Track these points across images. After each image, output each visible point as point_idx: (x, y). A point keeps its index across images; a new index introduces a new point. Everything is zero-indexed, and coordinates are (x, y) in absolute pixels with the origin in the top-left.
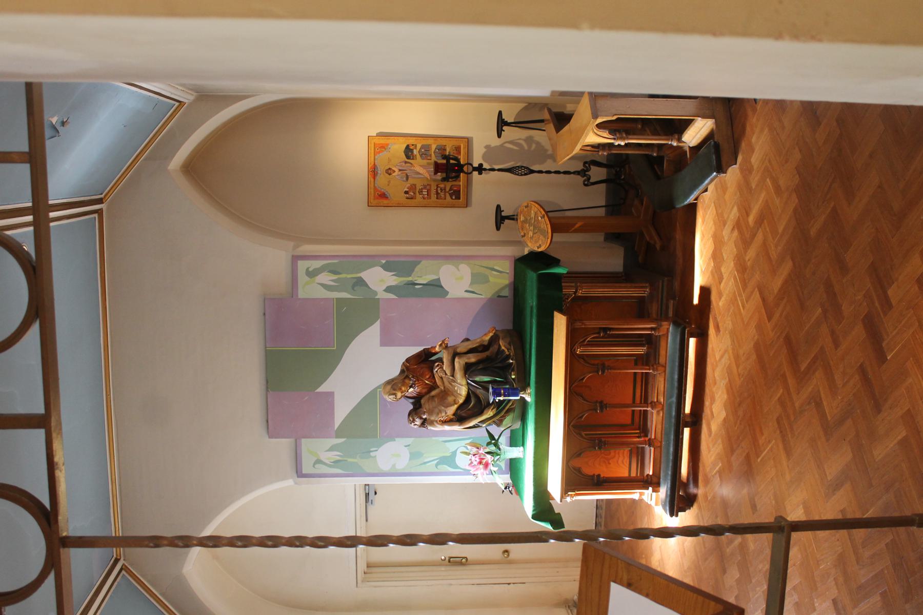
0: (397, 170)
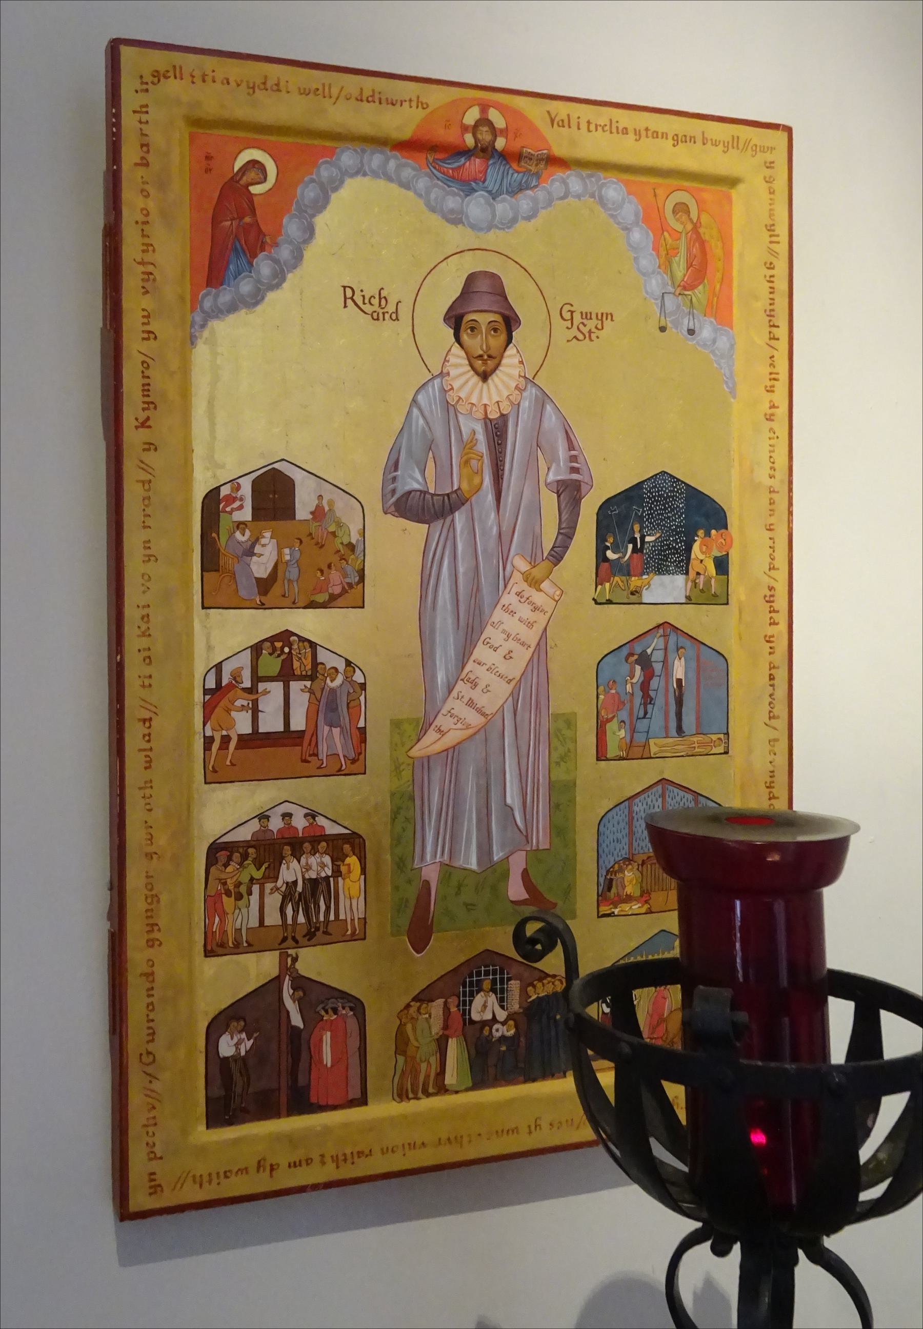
0: (499, 391)
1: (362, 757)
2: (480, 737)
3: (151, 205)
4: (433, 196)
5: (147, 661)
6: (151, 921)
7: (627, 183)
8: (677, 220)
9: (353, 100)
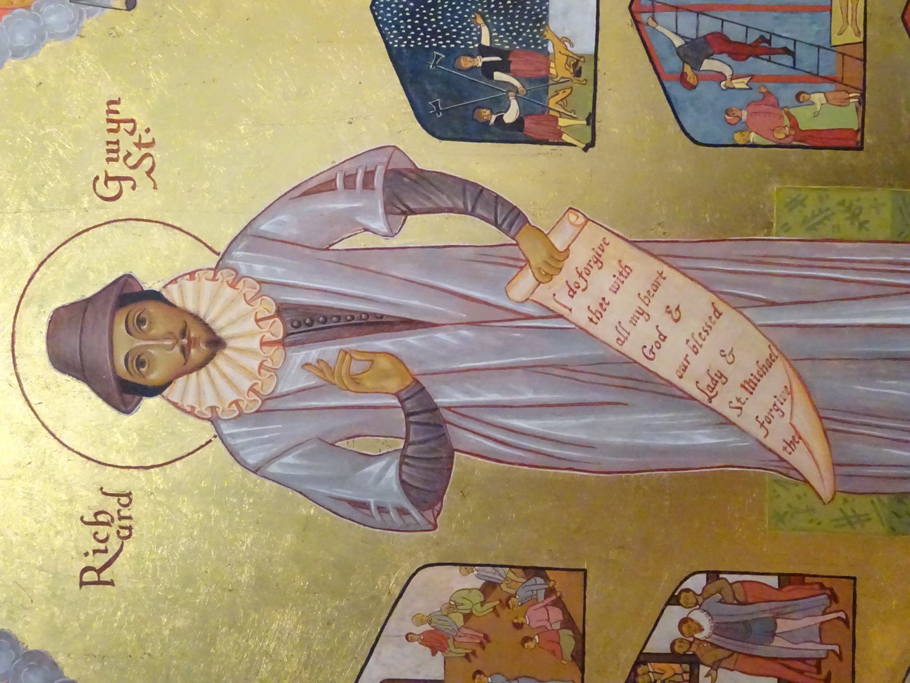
1: (827, 583)
2: (805, 368)
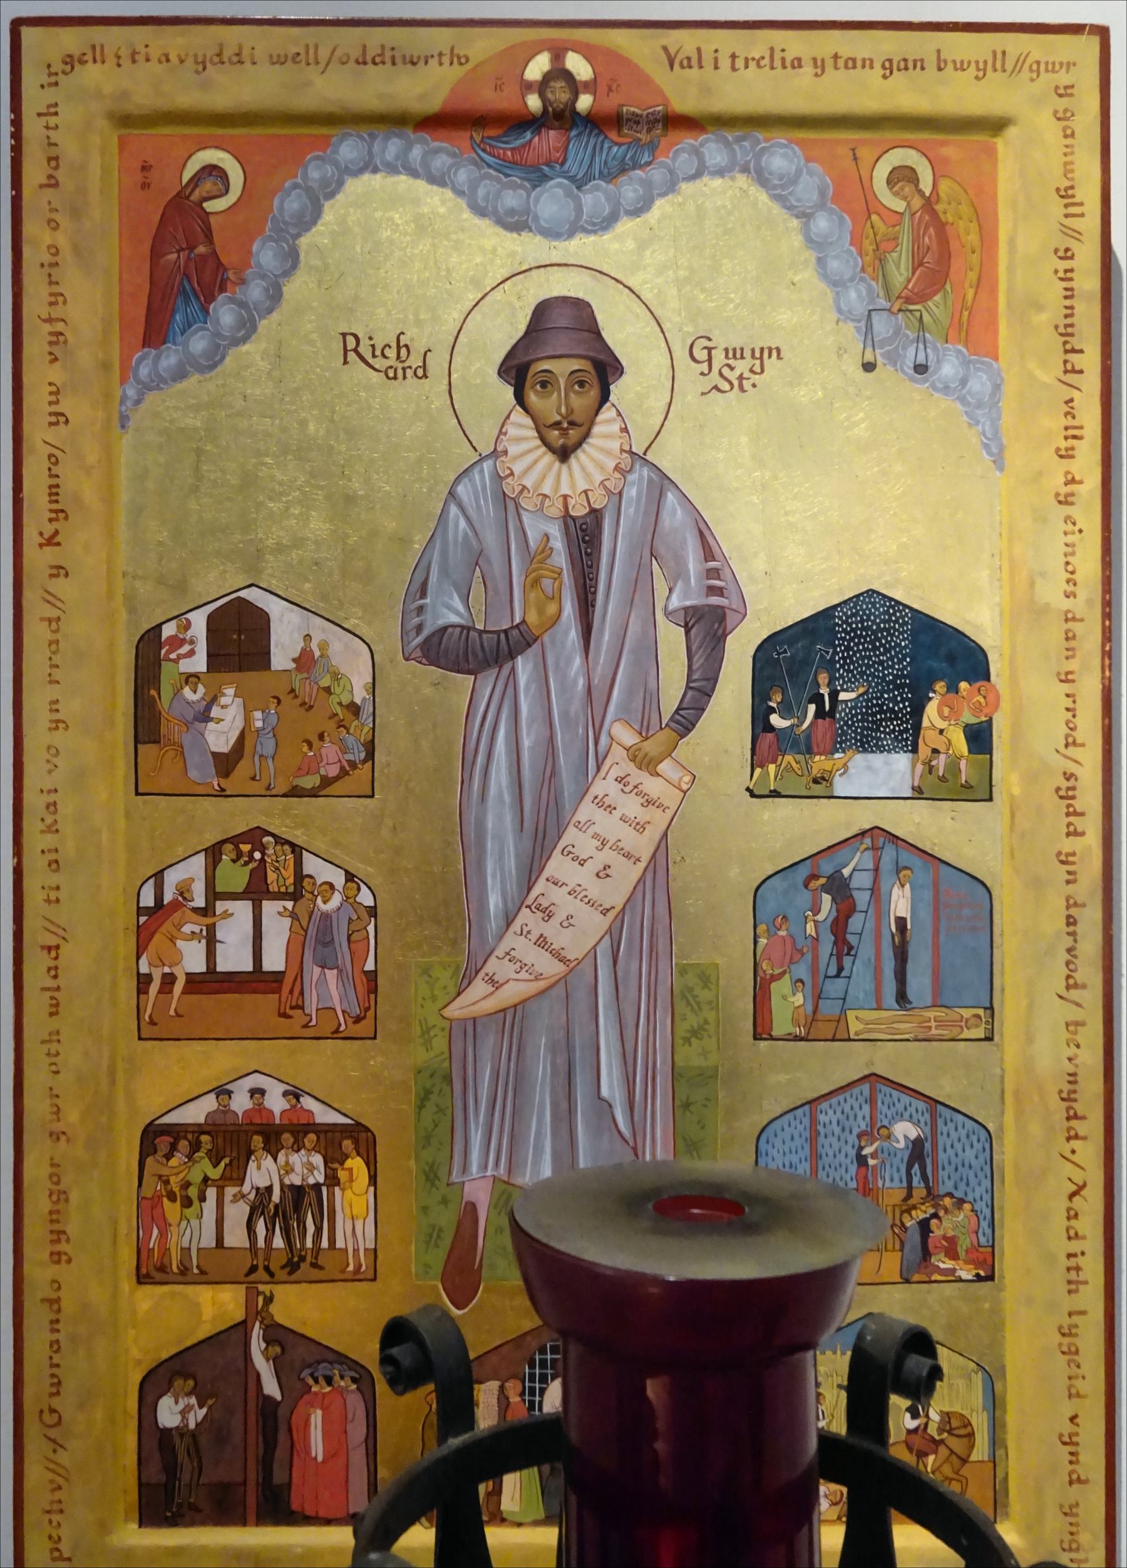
0: (587, 475)
2: (560, 990)
3: (62, 239)
4: (481, 192)
5: (54, 866)
6: (56, 1227)
7: (800, 143)
8: (896, 194)
9: (352, 64)
